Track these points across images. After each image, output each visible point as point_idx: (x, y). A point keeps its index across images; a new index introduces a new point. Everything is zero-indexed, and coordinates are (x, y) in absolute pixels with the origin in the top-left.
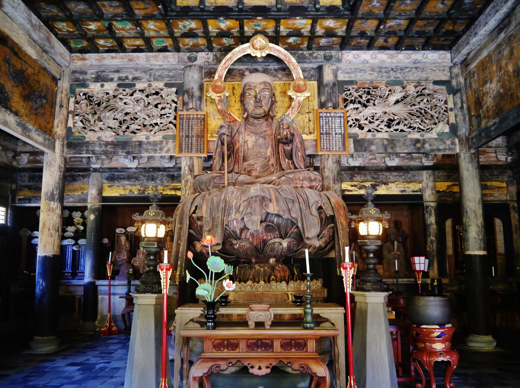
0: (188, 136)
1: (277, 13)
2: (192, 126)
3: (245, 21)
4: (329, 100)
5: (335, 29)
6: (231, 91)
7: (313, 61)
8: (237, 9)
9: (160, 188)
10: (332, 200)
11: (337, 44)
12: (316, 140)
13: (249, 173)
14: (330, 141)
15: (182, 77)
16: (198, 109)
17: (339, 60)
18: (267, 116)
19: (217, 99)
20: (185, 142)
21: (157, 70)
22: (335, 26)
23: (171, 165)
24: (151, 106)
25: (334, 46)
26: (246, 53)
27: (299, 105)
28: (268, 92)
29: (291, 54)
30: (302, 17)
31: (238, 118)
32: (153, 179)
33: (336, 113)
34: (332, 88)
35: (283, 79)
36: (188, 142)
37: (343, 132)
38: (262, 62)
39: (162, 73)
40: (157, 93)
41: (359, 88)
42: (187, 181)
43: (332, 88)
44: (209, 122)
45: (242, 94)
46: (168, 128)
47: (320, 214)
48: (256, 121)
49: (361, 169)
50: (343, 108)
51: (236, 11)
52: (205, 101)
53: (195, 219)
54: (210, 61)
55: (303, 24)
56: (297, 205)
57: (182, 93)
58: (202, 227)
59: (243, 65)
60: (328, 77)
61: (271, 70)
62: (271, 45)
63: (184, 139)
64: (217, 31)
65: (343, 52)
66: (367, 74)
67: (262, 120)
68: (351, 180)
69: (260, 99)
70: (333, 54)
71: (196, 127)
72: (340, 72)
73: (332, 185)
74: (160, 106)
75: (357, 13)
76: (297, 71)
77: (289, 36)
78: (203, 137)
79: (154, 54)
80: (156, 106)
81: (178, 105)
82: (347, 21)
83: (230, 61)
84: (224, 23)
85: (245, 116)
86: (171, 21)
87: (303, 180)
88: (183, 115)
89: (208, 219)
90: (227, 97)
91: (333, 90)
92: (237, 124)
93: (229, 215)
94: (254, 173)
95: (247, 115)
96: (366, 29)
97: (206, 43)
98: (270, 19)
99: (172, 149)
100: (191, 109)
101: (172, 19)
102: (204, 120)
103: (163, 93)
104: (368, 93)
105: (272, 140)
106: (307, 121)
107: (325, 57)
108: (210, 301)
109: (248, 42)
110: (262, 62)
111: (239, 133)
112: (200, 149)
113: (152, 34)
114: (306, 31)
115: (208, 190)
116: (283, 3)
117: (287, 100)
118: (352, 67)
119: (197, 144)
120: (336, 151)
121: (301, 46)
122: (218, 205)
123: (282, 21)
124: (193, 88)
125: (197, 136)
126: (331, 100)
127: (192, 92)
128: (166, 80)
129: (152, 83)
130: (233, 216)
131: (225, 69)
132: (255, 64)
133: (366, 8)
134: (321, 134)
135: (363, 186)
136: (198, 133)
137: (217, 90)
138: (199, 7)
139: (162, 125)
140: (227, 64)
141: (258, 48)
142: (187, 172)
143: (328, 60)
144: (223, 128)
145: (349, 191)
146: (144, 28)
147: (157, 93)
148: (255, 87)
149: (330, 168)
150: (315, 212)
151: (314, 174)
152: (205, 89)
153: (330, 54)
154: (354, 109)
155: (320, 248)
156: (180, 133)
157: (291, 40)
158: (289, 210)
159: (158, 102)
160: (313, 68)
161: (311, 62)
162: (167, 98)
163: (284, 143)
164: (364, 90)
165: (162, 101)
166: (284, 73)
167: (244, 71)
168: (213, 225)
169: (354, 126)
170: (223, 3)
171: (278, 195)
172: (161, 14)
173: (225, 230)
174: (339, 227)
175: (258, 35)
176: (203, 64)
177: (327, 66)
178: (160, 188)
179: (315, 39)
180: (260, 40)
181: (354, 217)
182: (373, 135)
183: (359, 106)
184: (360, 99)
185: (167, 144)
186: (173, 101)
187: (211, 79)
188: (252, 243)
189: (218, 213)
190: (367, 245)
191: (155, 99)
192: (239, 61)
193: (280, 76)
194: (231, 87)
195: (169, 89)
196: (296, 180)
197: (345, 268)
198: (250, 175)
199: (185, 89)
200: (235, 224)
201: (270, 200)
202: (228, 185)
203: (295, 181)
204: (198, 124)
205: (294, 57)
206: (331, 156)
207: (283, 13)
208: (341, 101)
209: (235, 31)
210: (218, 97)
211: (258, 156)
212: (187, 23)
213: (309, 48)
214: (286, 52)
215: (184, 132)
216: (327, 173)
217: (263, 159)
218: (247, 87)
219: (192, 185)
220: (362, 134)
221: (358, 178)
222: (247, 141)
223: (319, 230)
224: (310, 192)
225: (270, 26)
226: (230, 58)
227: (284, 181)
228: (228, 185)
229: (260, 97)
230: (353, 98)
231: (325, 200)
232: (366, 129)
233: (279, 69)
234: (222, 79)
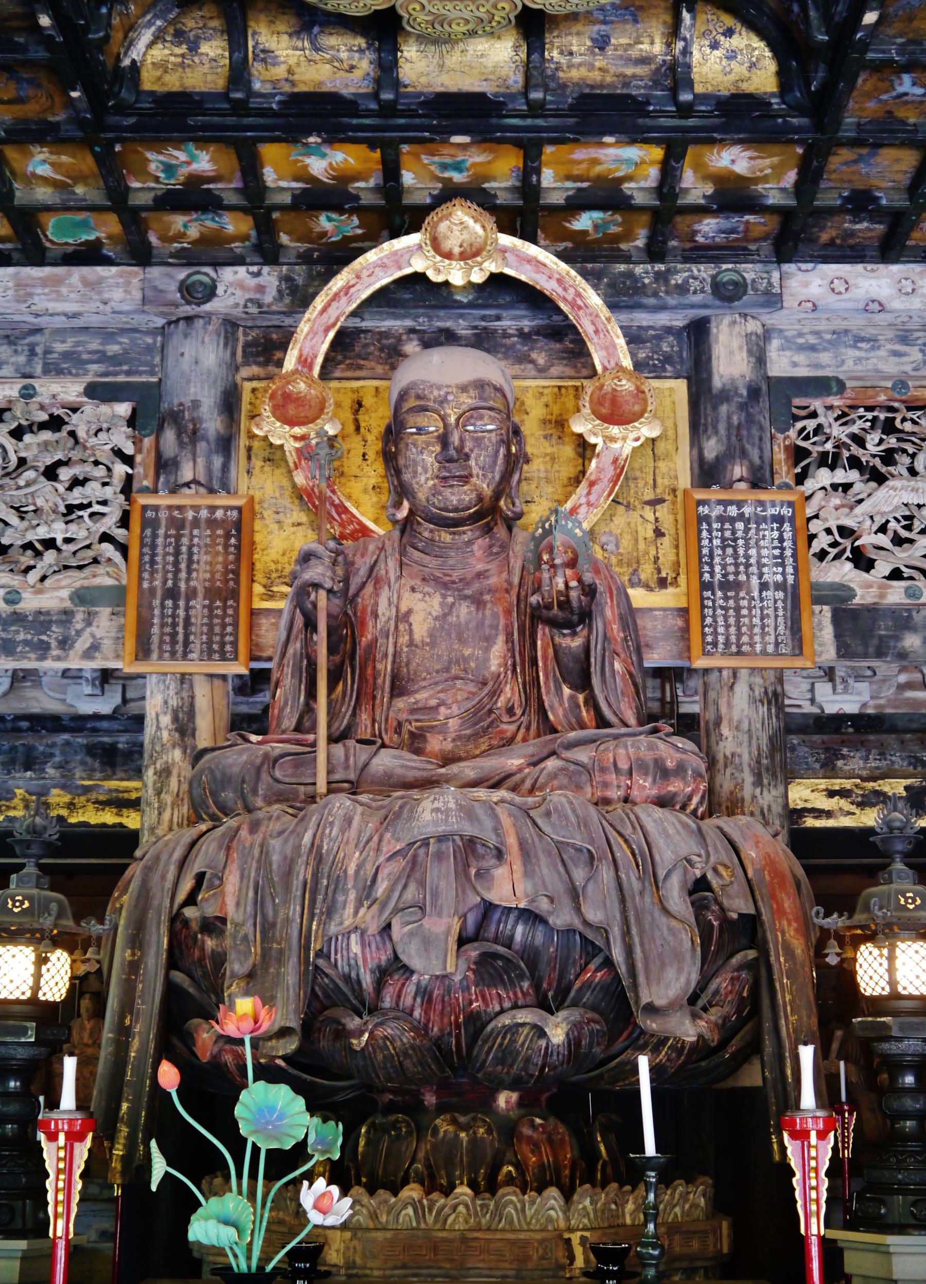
0: (172, 594)
1: (529, 122)
2: (190, 554)
3: (405, 148)
5: (755, 180)
6: (348, 415)
7: (672, 301)
8: (373, 106)
9: (57, 797)
10: (750, 853)
11: (764, 239)
12: (684, 612)
13: (415, 742)
14: (738, 616)
15: (157, 360)
16: (221, 483)
17: (773, 300)
18: (491, 516)
19: (291, 446)
20: (163, 616)
21: (61, 333)
22: (752, 169)
23: (105, 706)
24: (30, 474)
25: (753, 247)
26: (408, 271)
27: (617, 476)
28: (493, 420)
29: (584, 274)
30: (623, 137)
31: (376, 521)
32: (31, 762)
33: (761, 503)
34: (743, 407)
35: (554, 371)
36: (174, 616)
37: (790, 579)
38: (471, 305)
39: (78, 344)
40: (55, 423)
41: (854, 407)
42: (165, 773)
43: (743, 407)
44: (258, 538)
45: (388, 429)
46: (96, 561)
47: (699, 908)
49: (864, 727)
50: (792, 483)
51: (369, 114)
52: (243, 453)
53: (195, 926)
54: (268, 298)
55: (631, 162)
56: (606, 873)
57: (155, 423)
58: (219, 959)
59: (396, 317)
60: (730, 362)
61: (506, 335)
62: (505, 240)
63: (157, 602)
64: (295, 185)
65: (786, 267)
66: (882, 353)
67: (468, 533)
68: (829, 769)
69: (460, 450)
70: (749, 276)
71: (205, 558)
72: (775, 343)
73: (748, 791)
74: (65, 474)
75: (838, 123)
76: (609, 343)
77: (576, 205)
78: (234, 594)
79: (47, 271)
80: (51, 473)
81: (139, 470)
82: (800, 151)
83: (344, 300)
84: (323, 156)
85: (403, 513)
86: (118, 148)
87: (630, 773)
88: (156, 508)
89: (248, 928)
90: (332, 440)
91: (748, 414)
92: (371, 547)
93: (330, 912)
94: (435, 743)
95: (411, 512)
96: (875, 182)
97: (253, 233)
98: (501, 141)
99: (107, 645)
100: (187, 485)
101: (122, 141)
102: (239, 530)
103: (79, 423)
104: (889, 428)
105: (508, 612)
106: (650, 534)
108: (244, 1268)
110: (471, 305)
111: (378, 583)
112: (223, 644)
113: (43, 194)
114: (642, 185)
115: (249, 810)
116: (552, 85)
117: (568, 451)
118: (822, 326)
119: (211, 626)
120: (764, 653)
121: (623, 246)
122: (288, 873)
123: (549, 150)
124: (196, 404)
125: (211, 593)
126: (744, 454)
127: (193, 420)
128: (94, 372)
129: (36, 383)
130: (347, 916)
131: (327, 331)
132: (442, 313)
133: (871, 105)
134: (706, 586)
135: (878, 793)
136: (212, 580)
137: (291, 411)
138: (224, 96)
139: (72, 547)
140: (333, 312)
141: (457, 250)
142: (165, 735)
144: (313, 561)
145: (819, 813)
146: (13, 173)
147: (55, 423)
148: (443, 401)
149: (741, 722)
150: (676, 897)
151: (674, 749)
152: (245, 407)
153: (735, 277)
154: (835, 487)
155: (701, 1049)
156: (141, 579)
157: (584, 222)
158: (575, 895)
159: (59, 456)
160: (669, 330)
161: (663, 308)
162: (93, 441)
163: (555, 624)
164: (869, 416)
165: (75, 455)
166: (558, 346)
167: (399, 339)
168: (265, 953)
169: (837, 557)
170: (321, 83)
171: (529, 832)
172: (80, 123)
173: (312, 975)
174: (779, 962)
175: (457, 202)
176: (238, 312)
177: (727, 320)
178: (57, 797)
179: (678, 219)
180: (463, 223)
181: (835, 921)
182: (912, 593)
183: (853, 475)
184: (856, 450)
185: (89, 623)
186: (118, 453)
187: (271, 369)
188: (421, 1030)
189: (286, 902)
190: (889, 1039)
191: (45, 446)
192: (383, 299)
194: (347, 402)
195: (105, 409)
196: (603, 770)
197: (801, 1135)
198: (418, 752)
199: (165, 406)
200: (355, 948)
201: (500, 854)
202: (330, 791)
203: (598, 778)
205: (596, 287)
206: (743, 674)
207: (552, 121)
208: (780, 456)
209: (365, 188)
210: (296, 438)
211: (450, 673)
212: (182, 156)
213: (654, 252)
214: (563, 266)
215: (159, 576)
216: (729, 743)
217: (472, 688)
218: (412, 403)
219: (185, 787)
220: (865, 588)
221: (855, 762)
222: (409, 612)
223: (695, 977)
224: (659, 822)
225: (502, 170)
226: (347, 289)
227: (554, 776)
228: (330, 791)
229: (462, 440)
230: (829, 446)
231: (721, 853)
232: (883, 568)
233: (538, 331)
234: (311, 368)
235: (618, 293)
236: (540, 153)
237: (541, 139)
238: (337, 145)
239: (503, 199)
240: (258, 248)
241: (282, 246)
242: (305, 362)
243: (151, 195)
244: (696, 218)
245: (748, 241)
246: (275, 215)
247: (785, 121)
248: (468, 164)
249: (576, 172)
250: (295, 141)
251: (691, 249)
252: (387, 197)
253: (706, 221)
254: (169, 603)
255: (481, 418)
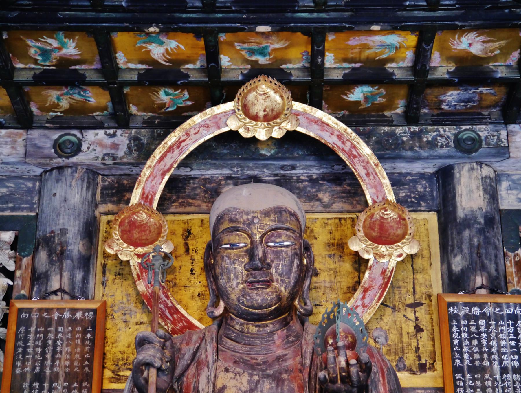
0: (39, 378)
1: (315, 15)
2: (55, 346)
3: (223, 37)
4: (476, 265)
5: (487, 60)
6: (180, 241)
7: (424, 153)
11: (494, 106)
15: (36, 199)
17: (502, 152)
18: (287, 312)
19: (135, 262)
22: (485, 51)
25: (485, 113)
26: (225, 129)
28: (289, 238)
29: (359, 133)
31: (200, 320)
33: (499, 305)
34: (481, 231)
35: (336, 206)
38: (272, 158)
43: (481, 231)
44: (109, 334)
45: (209, 247)
48: (253, 329)
54: (120, 153)
57: (32, 247)
59: (217, 167)
60: (470, 197)
61: (299, 180)
62: (298, 106)
63: (26, 385)
64: (140, 66)
65: (511, 127)
67: (270, 326)
69: (263, 260)
70: (483, 135)
76: (378, 185)
77: (352, 80)
78: (89, 378)
81: (18, 282)
83: (177, 151)
84: (161, 43)
88: (30, 311)
90: (166, 257)
91: (486, 238)
92: (195, 338)
97: (110, 105)
98: (294, 30)
100: (55, 293)
101: (8, 29)
102: (94, 327)
106: (412, 330)
107: (459, 142)
109: (230, 98)
110: (272, 158)
111: (199, 364)
114: (400, 67)
117: (347, 266)
121: (387, 113)
123: (331, 37)
124: (64, 232)
125: (70, 377)
126: (483, 268)
127: (61, 244)
131: (163, 174)
132: (251, 164)
134: (457, 370)
136: (71, 366)
137: (136, 235)
140: (168, 161)
141: (261, 114)
143: (469, 151)
144: (146, 346)
148: (250, 223)
152: (102, 234)
156: (14, 367)
157: (357, 94)
160: (422, 176)
166: (338, 188)
167: (219, 184)
175: (261, 78)
176: (98, 163)
177: (467, 167)
179: (428, 91)
180: (266, 94)
192: (205, 152)
193: (326, 198)
194: (179, 230)
199: (40, 233)
204: (74, 338)
205: (368, 143)
207: (333, 15)
209: (193, 69)
210: (139, 256)
212: (55, 44)
213: (411, 117)
214: (342, 125)
215: (29, 364)
218: (226, 225)
226: (179, 143)
229: (265, 253)
233: (323, 178)
234: (151, 203)
235: (384, 148)
236: (324, 40)
237: (325, 27)
238: (171, 34)
239: (296, 76)
240: (113, 116)
241: (131, 115)
242: (147, 198)
243: (32, 73)
244: (442, 90)
245: (482, 108)
246: (126, 90)
247: (510, 11)
248: (269, 50)
249: (350, 56)
250: (140, 30)
251: (438, 115)
252: (209, 76)
253: (450, 93)
254: (36, 385)
255: (280, 236)
